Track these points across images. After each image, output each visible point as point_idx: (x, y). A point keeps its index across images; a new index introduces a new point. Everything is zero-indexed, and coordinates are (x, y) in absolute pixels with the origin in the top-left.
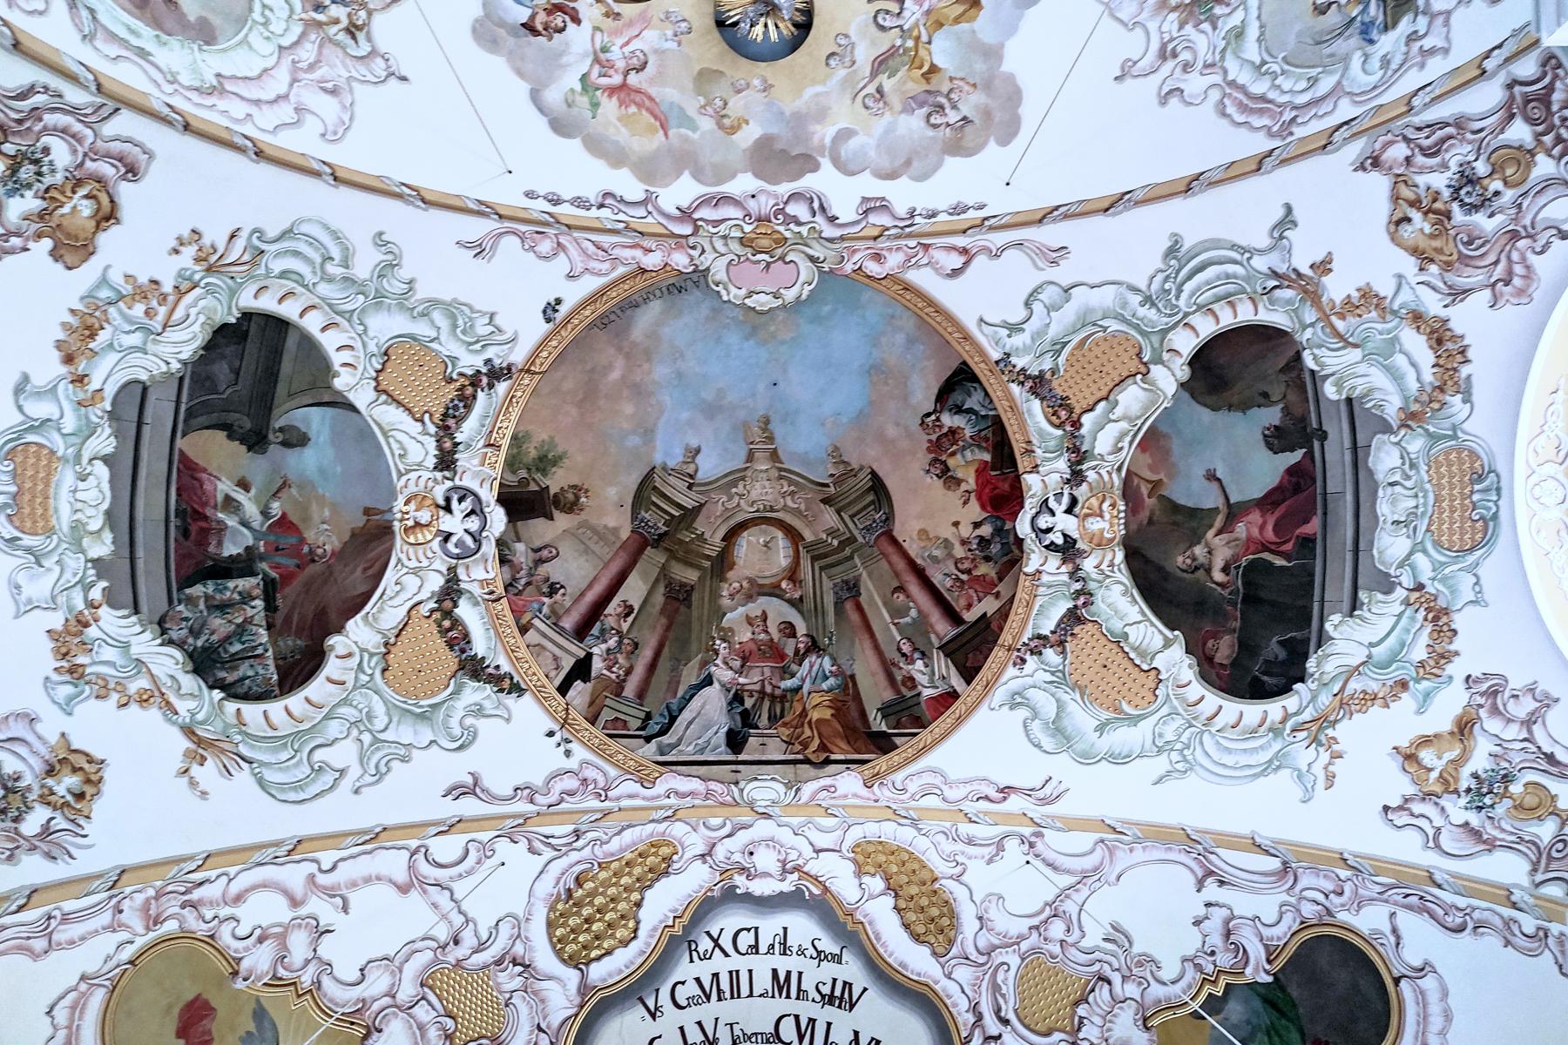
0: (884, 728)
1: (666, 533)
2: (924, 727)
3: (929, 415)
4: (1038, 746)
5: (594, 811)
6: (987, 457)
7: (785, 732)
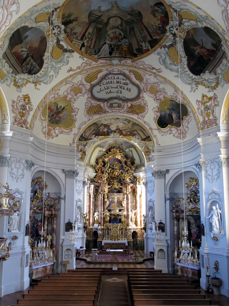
0: (136, 53)
1: (95, 20)
2: (143, 54)
3: (153, 6)
4: (160, 63)
5: (89, 68)
6: (163, 16)
7: (119, 52)
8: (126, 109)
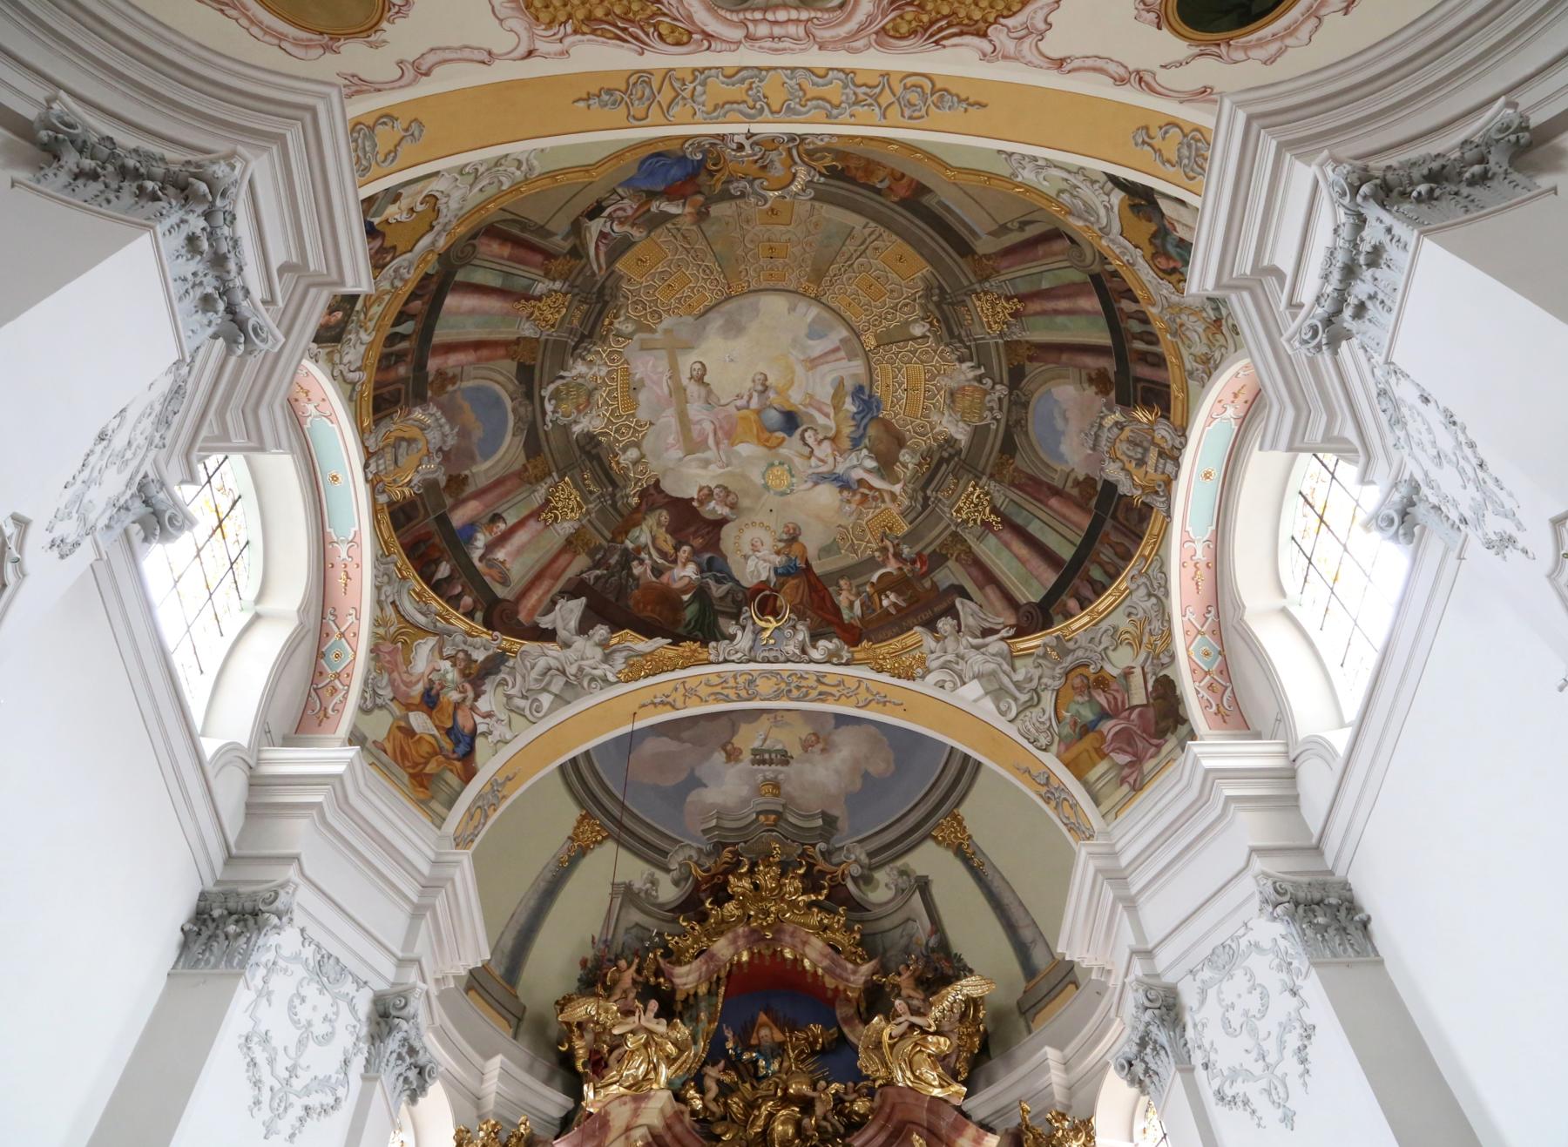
8: (871, 19)
